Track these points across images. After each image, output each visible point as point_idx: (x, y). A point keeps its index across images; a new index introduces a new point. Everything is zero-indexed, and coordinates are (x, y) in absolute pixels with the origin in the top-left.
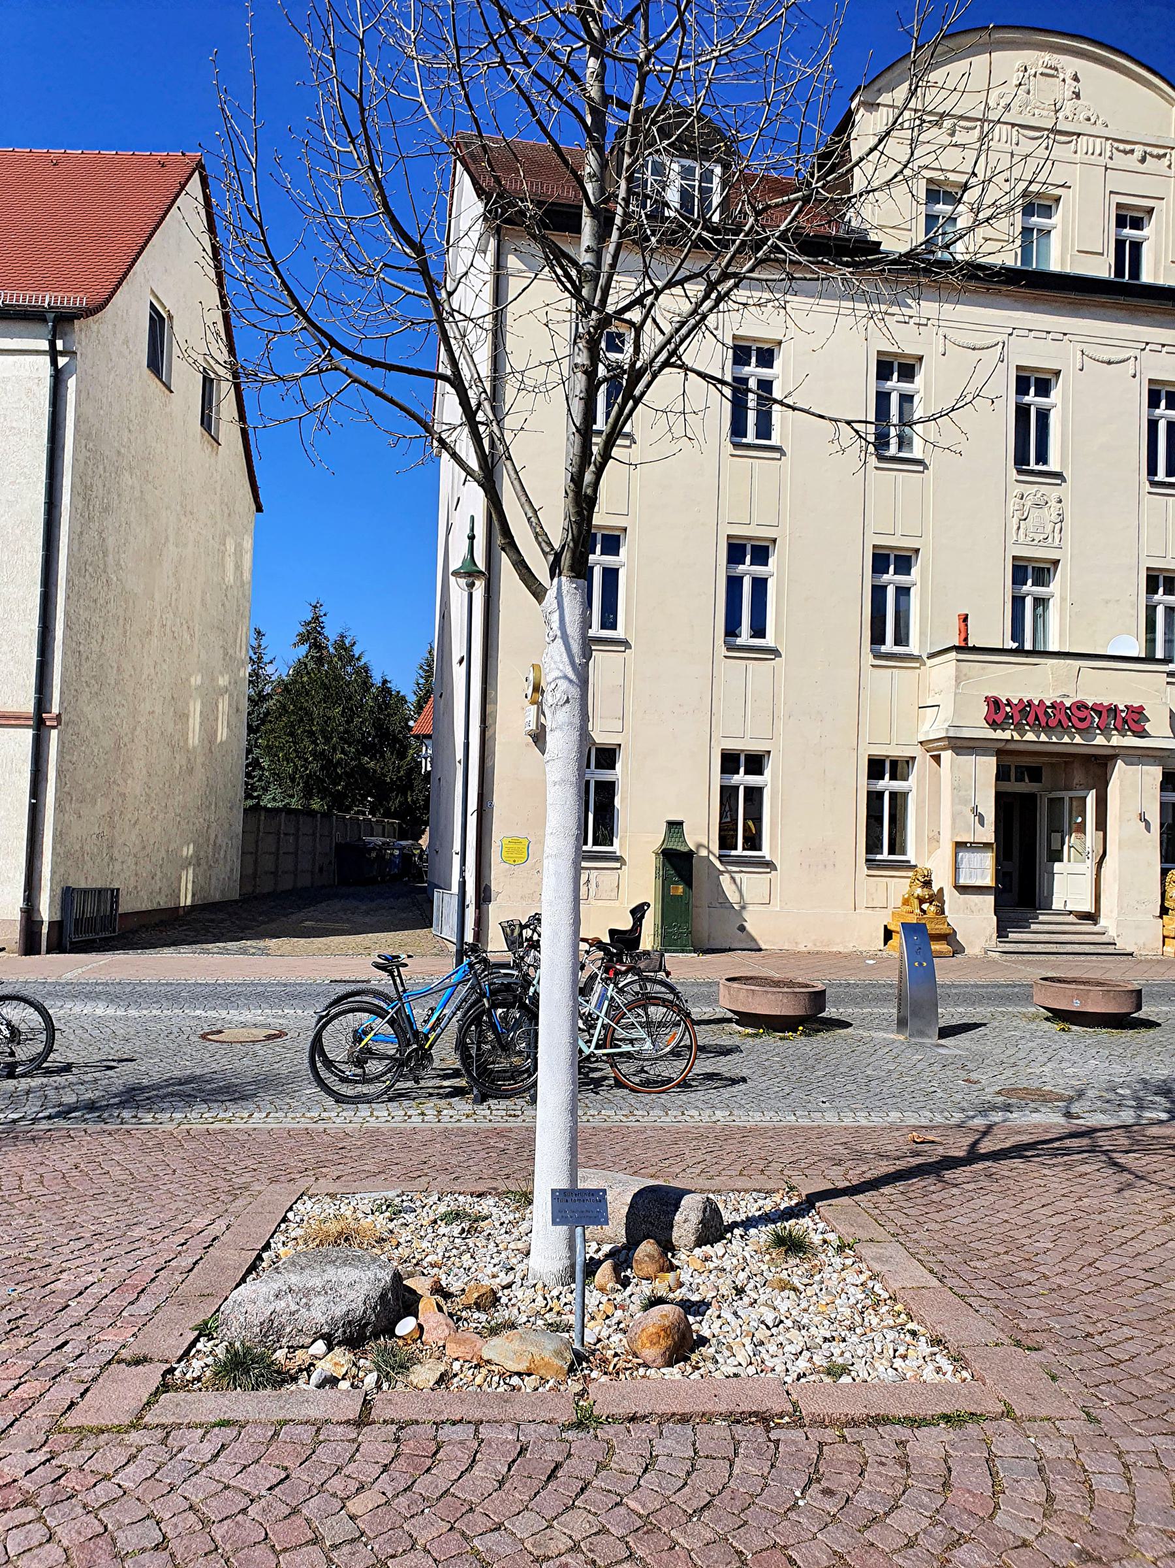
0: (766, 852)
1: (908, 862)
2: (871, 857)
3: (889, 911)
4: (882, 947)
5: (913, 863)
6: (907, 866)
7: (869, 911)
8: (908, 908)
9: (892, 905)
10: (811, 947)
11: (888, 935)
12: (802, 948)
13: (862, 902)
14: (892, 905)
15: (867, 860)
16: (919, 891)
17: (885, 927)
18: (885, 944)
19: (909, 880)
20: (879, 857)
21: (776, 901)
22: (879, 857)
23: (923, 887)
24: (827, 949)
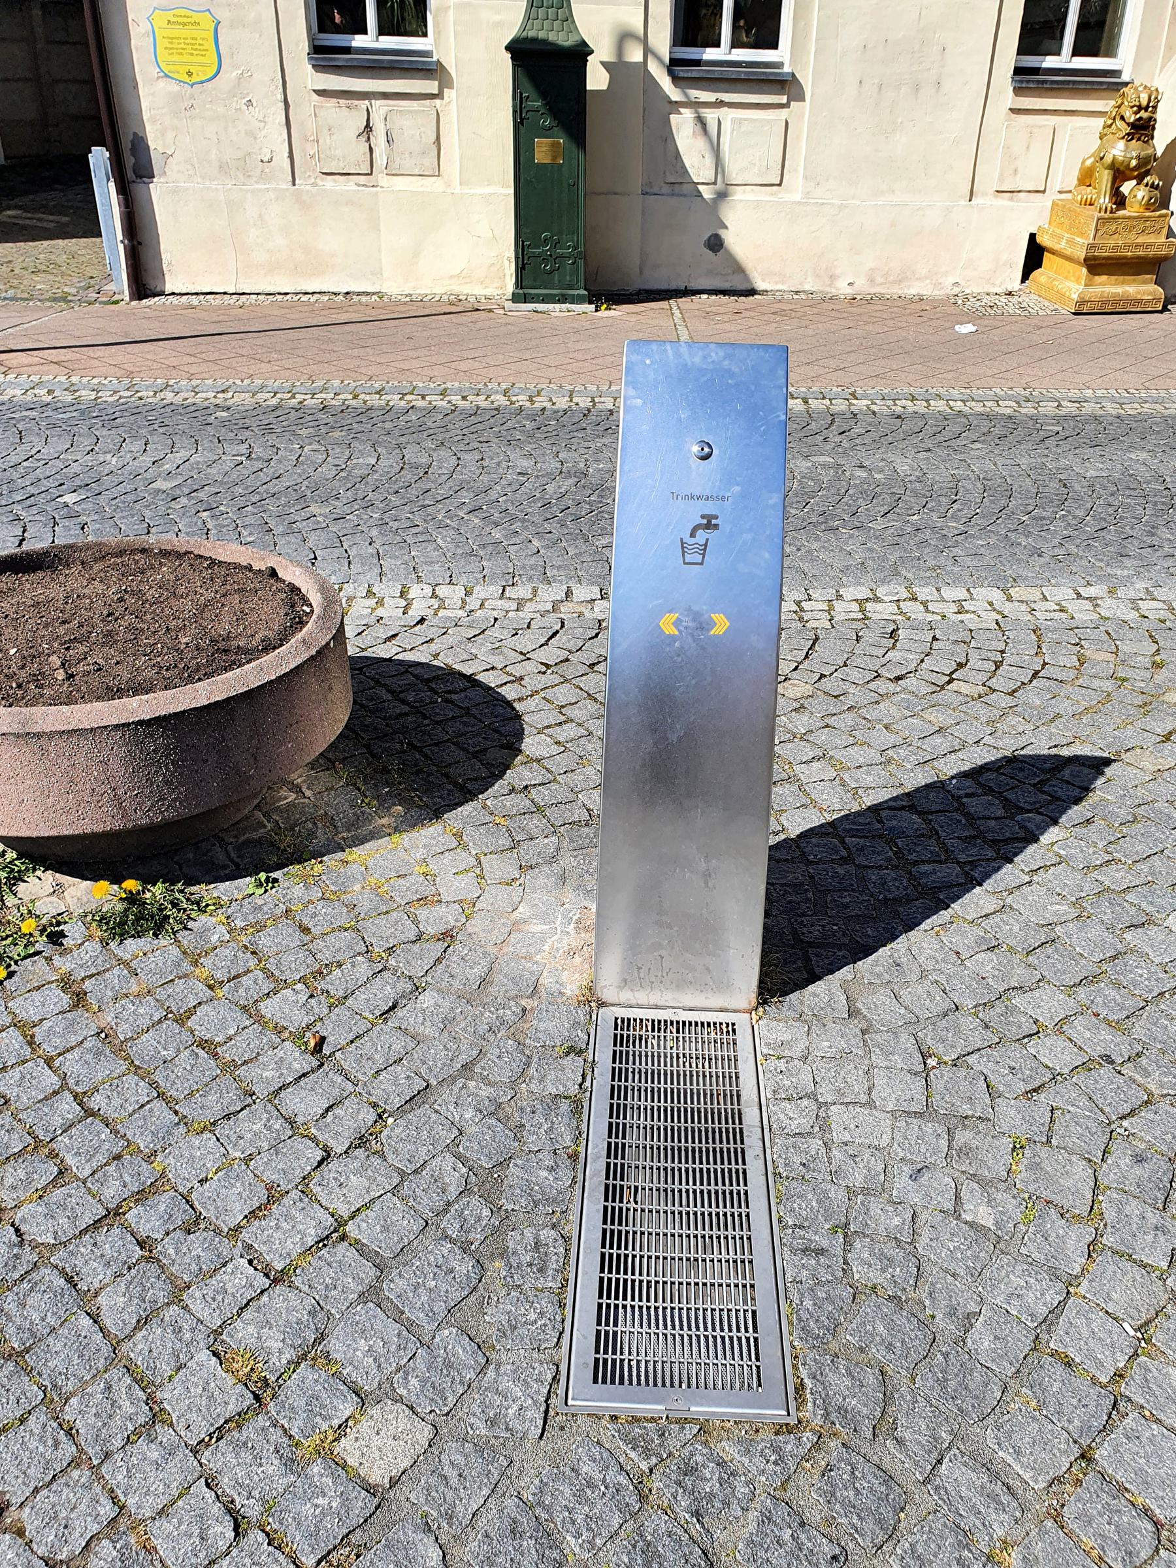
0: (781, 55)
1: (1116, 73)
2: (1031, 61)
3: (1046, 201)
4: (1015, 284)
5: (1125, 77)
6: (1109, 83)
7: (1004, 201)
8: (1088, 193)
9: (1056, 184)
10: (862, 286)
11: (1035, 255)
12: (842, 288)
13: (988, 180)
14: (1056, 184)
15: (1018, 71)
16: (1119, 150)
17: (1032, 237)
18: (1025, 277)
19: (1100, 122)
20: (1050, 62)
21: (795, 179)
22: (1050, 62)
23: (1130, 137)
24: (896, 291)
